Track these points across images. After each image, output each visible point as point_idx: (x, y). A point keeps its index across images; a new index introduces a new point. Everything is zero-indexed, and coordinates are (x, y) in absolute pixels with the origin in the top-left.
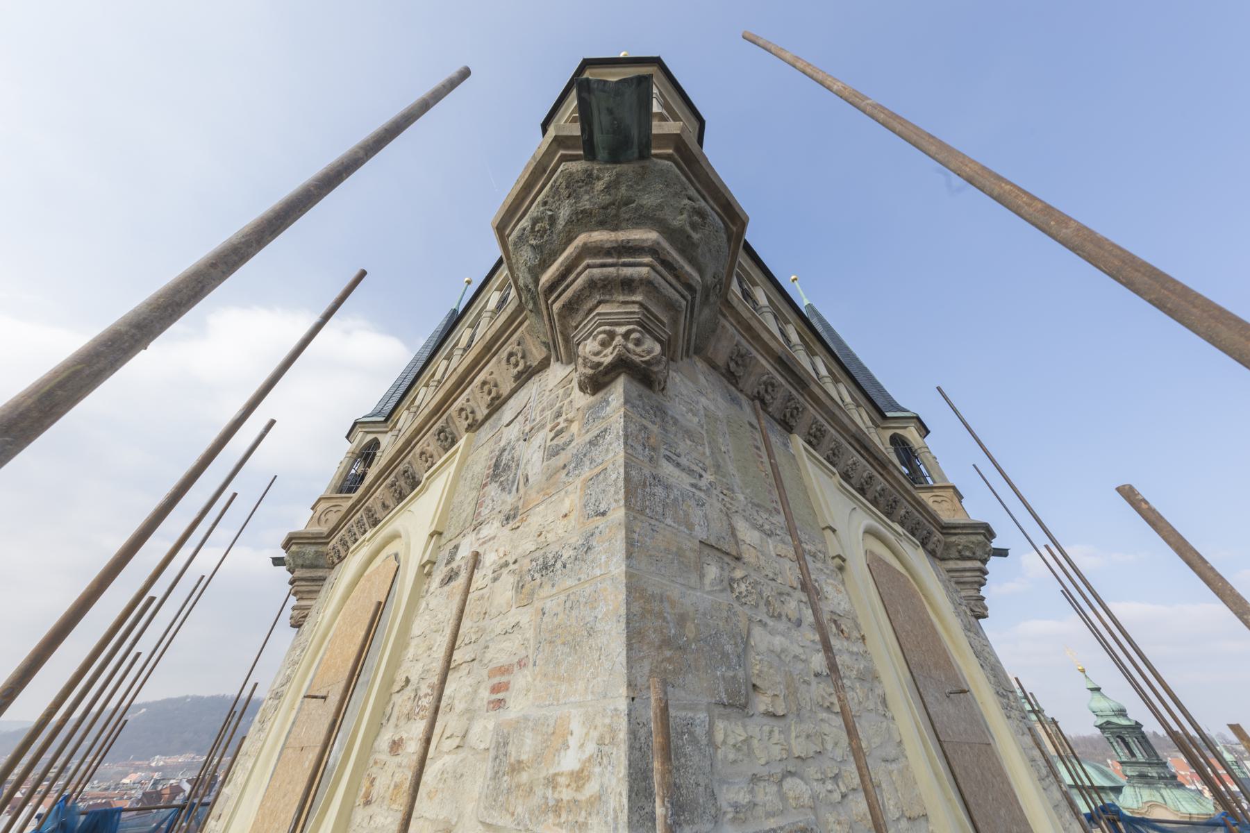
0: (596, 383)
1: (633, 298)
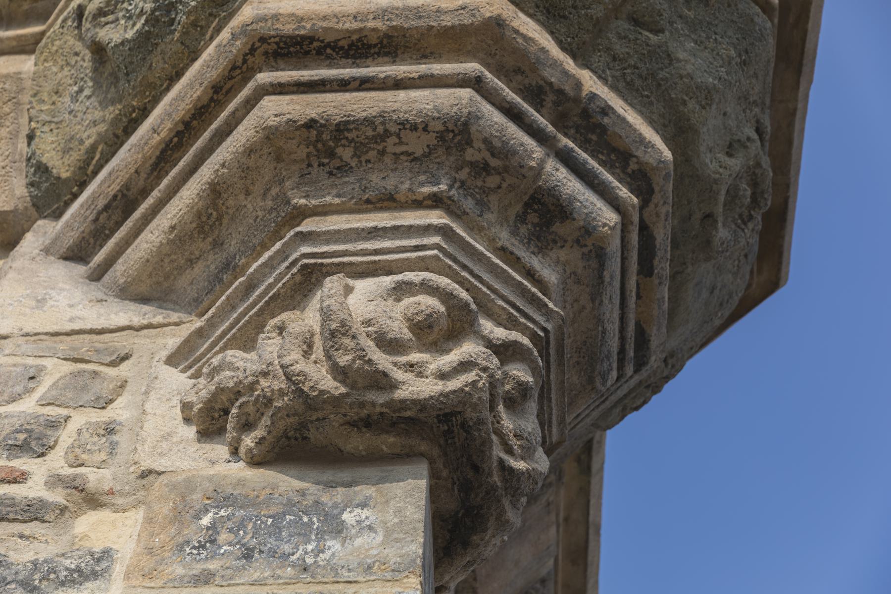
0: (317, 435)
1: (535, 263)
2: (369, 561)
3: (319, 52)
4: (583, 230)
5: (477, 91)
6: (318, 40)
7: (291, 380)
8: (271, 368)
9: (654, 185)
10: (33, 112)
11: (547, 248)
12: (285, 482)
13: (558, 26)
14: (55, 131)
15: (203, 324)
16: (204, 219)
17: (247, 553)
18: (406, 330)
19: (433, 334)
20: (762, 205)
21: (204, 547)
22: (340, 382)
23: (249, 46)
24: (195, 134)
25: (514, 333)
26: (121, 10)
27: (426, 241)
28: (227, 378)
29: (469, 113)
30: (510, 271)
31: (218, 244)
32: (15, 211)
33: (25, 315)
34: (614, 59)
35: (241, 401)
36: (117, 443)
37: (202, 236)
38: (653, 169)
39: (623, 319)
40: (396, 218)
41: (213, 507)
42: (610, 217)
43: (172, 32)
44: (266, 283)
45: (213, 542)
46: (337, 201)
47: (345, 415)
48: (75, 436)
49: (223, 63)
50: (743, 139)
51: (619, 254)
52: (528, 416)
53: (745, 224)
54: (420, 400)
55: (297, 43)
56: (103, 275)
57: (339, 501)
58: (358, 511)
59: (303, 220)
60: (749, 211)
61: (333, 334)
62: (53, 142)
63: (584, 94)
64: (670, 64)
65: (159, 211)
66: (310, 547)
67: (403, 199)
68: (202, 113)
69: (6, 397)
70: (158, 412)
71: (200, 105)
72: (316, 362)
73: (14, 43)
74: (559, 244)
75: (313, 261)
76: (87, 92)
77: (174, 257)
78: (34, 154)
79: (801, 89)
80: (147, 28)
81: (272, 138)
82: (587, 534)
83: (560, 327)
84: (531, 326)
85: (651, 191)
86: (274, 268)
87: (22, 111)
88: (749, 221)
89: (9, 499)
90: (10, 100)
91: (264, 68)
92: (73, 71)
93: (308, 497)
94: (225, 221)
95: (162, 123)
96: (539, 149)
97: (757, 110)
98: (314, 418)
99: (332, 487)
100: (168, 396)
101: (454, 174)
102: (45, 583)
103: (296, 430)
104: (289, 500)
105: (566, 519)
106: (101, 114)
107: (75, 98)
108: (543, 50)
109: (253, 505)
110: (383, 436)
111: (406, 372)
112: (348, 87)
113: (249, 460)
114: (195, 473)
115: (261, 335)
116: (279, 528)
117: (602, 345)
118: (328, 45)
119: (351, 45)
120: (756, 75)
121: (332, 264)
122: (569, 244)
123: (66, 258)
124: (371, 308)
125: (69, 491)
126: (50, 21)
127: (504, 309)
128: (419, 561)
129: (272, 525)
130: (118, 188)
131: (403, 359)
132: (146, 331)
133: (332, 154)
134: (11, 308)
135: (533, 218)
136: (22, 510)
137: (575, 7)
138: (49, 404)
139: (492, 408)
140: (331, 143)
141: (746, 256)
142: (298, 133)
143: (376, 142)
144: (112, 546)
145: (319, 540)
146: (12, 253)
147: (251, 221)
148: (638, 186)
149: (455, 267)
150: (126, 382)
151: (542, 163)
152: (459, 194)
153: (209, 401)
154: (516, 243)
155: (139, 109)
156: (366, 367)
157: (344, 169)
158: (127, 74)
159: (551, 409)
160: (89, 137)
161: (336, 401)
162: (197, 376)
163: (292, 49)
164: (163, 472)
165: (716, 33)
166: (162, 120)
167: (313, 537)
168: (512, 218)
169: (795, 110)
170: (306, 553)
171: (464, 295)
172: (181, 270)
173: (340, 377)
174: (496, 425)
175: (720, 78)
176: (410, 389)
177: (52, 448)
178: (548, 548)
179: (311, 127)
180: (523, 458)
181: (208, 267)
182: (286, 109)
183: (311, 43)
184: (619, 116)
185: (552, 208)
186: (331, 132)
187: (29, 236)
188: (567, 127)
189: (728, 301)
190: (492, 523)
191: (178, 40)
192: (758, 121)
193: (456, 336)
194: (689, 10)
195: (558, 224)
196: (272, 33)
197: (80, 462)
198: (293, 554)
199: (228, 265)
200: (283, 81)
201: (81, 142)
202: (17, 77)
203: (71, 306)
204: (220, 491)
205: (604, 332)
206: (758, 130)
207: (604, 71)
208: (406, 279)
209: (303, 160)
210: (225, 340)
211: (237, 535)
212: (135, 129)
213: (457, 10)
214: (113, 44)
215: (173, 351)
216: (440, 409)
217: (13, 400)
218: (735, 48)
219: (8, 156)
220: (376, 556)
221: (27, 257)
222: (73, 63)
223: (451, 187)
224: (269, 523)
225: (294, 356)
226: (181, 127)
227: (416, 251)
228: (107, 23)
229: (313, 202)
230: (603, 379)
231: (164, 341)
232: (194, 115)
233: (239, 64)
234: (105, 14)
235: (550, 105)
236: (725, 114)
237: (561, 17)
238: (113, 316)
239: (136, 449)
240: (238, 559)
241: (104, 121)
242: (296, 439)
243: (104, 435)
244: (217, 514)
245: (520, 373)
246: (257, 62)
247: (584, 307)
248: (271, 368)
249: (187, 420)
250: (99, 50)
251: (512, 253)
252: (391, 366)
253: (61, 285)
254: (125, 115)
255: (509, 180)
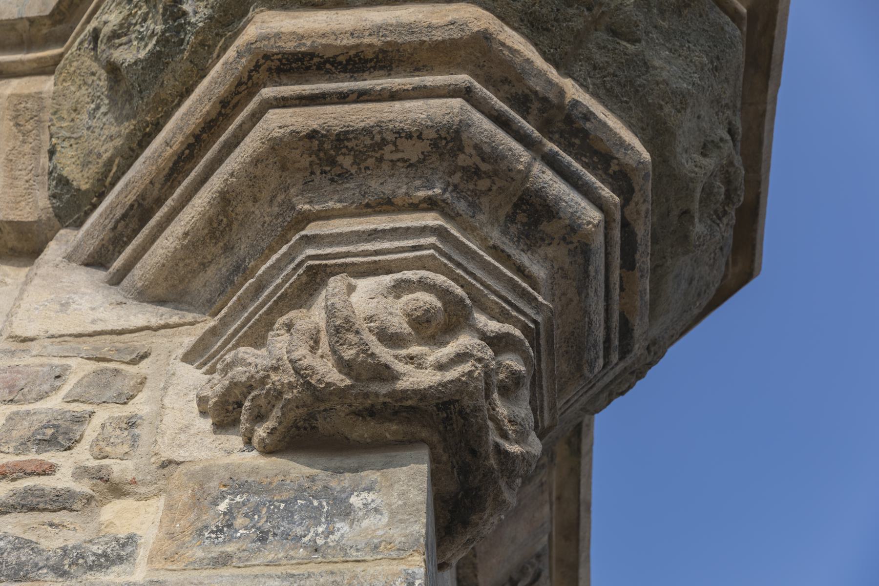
0: (325, 424)
1: (525, 259)
2: (376, 541)
3: (320, 67)
4: (568, 229)
5: (467, 101)
6: (318, 56)
7: (299, 374)
8: (280, 363)
9: (634, 185)
10: (53, 129)
11: (535, 246)
12: (295, 469)
13: (541, 39)
14: (75, 146)
15: (216, 323)
16: (215, 225)
17: (262, 536)
18: (405, 325)
19: (431, 328)
20: (735, 201)
21: (221, 531)
22: (345, 374)
23: (254, 63)
24: (205, 146)
25: (506, 325)
26: (134, 32)
27: (423, 241)
28: (240, 373)
29: (461, 121)
30: (502, 268)
31: (228, 249)
32: (38, 222)
33: (50, 318)
34: (595, 68)
35: (253, 394)
36: (138, 436)
37: (214, 241)
38: (633, 170)
39: (608, 310)
40: (394, 220)
41: (229, 494)
42: (594, 215)
43: (182, 51)
44: (275, 284)
45: (229, 526)
46: (339, 206)
47: (350, 406)
48: (99, 430)
49: (230, 80)
50: (717, 139)
51: (603, 250)
52: (521, 402)
53: (720, 219)
54: (420, 390)
55: (301, 60)
56: (122, 280)
57: (347, 486)
58: (364, 494)
59: (307, 224)
60: (724, 207)
61: (337, 330)
62: (72, 157)
63: (567, 101)
64: (647, 72)
65: (173, 219)
66: (320, 530)
67: (400, 203)
68: (211, 126)
69: (34, 395)
70: (176, 406)
71: (209, 119)
72: (322, 357)
73: (35, 65)
74: (546, 242)
75: (317, 262)
76: (103, 109)
77: (187, 261)
78: (55, 168)
79: (770, 92)
80: (158, 49)
81: (277, 149)
82: (578, 511)
83: (550, 319)
84: (523, 318)
85: (632, 191)
86: (281, 270)
87: (43, 128)
88: (723, 216)
89: (39, 490)
90: (31, 118)
91: (268, 83)
92: (90, 90)
93: (318, 483)
94: (235, 227)
95: (173, 137)
96: (526, 153)
97: (728, 113)
98: (322, 408)
99: (340, 473)
100: (185, 391)
101: (447, 178)
102: (74, 567)
103: (305, 420)
104: (300, 486)
105: (559, 498)
106: (117, 129)
107: (92, 115)
108: (528, 61)
109: (266, 491)
110: (387, 424)
111: (406, 364)
112: (347, 99)
113: (261, 449)
114: (212, 462)
115: (271, 333)
116: (291, 512)
117: (588, 335)
118: (327, 61)
119: (349, 60)
120: (727, 80)
121: (336, 265)
122: (556, 241)
123: (87, 265)
124: (373, 305)
125: (94, 481)
126: (68, 43)
127: (497, 303)
128: (422, 541)
129: (284, 509)
130: (135, 198)
131: (404, 352)
132: (163, 331)
133: (333, 162)
134: (37, 312)
135: (522, 217)
136: (51, 500)
137: (556, 20)
138: (74, 401)
139: (488, 396)
140: (332, 152)
141: (721, 249)
142: (301, 143)
143: (374, 150)
144: (136, 532)
145: (328, 523)
146: (36, 261)
147: (259, 226)
148: (620, 186)
149: (450, 265)
150: (146, 378)
151: (529, 166)
152: (452, 197)
153: (224, 395)
154: (507, 241)
155: (152, 124)
156: (369, 360)
157: (344, 176)
158: (141, 92)
159: (543, 396)
160: (106, 151)
161: (342, 392)
162: (211, 371)
163: (293, 65)
164: (182, 462)
165: (689, 42)
166: (174, 134)
167: (323, 520)
168: (502, 219)
169: (765, 111)
170: (317, 535)
171: (459, 291)
172: (194, 273)
173: (345, 370)
174: (492, 412)
175: (694, 84)
176: (411, 379)
177: (78, 441)
178: (543, 525)
179: (313, 137)
180: (517, 442)
181: (220, 270)
182: (289, 121)
183: (311, 59)
184: (600, 121)
185: (540, 208)
186: (332, 141)
187: (52, 245)
188: (552, 132)
189: (705, 291)
190: (489, 502)
191: (187, 59)
192: (730, 123)
193: (453, 330)
194: (664, 21)
195: (545, 223)
196: (275, 50)
197: (104, 454)
198: (305, 536)
199: (238, 267)
200: (286, 95)
201: (99, 156)
202: (38, 97)
203: (93, 309)
204: (235, 478)
205: (590, 322)
206: (730, 132)
207: (585, 79)
208: (405, 277)
209: (306, 169)
210: (237, 338)
211: (252, 519)
212: (149, 143)
213: (447, 25)
214: (126, 64)
215: (189, 349)
216: (439, 398)
217: (40, 397)
218: (707, 55)
219: (31, 171)
220: (382, 536)
221: (51, 264)
222: (90, 82)
223: (445, 190)
224: (282, 508)
225: (302, 351)
226: (192, 140)
227: (414, 251)
228: (121, 45)
229: (317, 207)
230: (590, 367)
231: (180, 340)
232: (203, 128)
233: (245, 80)
234: (119, 37)
235: (536, 112)
236: (699, 117)
237: (544, 30)
238: (132, 318)
239: (156, 441)
240: (254, 541)
241: (120, 136)
242: (305, 429)
243: (126, 429)
244: (233, 500)
245: (513, 362)
246: (261, 77)
247: (571, 300)
248: (280, 363)
249: (203, 413)
250: (113, 70)
251: (503, 251)
252: (392, 359)
253: (83, 289)
254: (140, 130)
255: (499, 183)
